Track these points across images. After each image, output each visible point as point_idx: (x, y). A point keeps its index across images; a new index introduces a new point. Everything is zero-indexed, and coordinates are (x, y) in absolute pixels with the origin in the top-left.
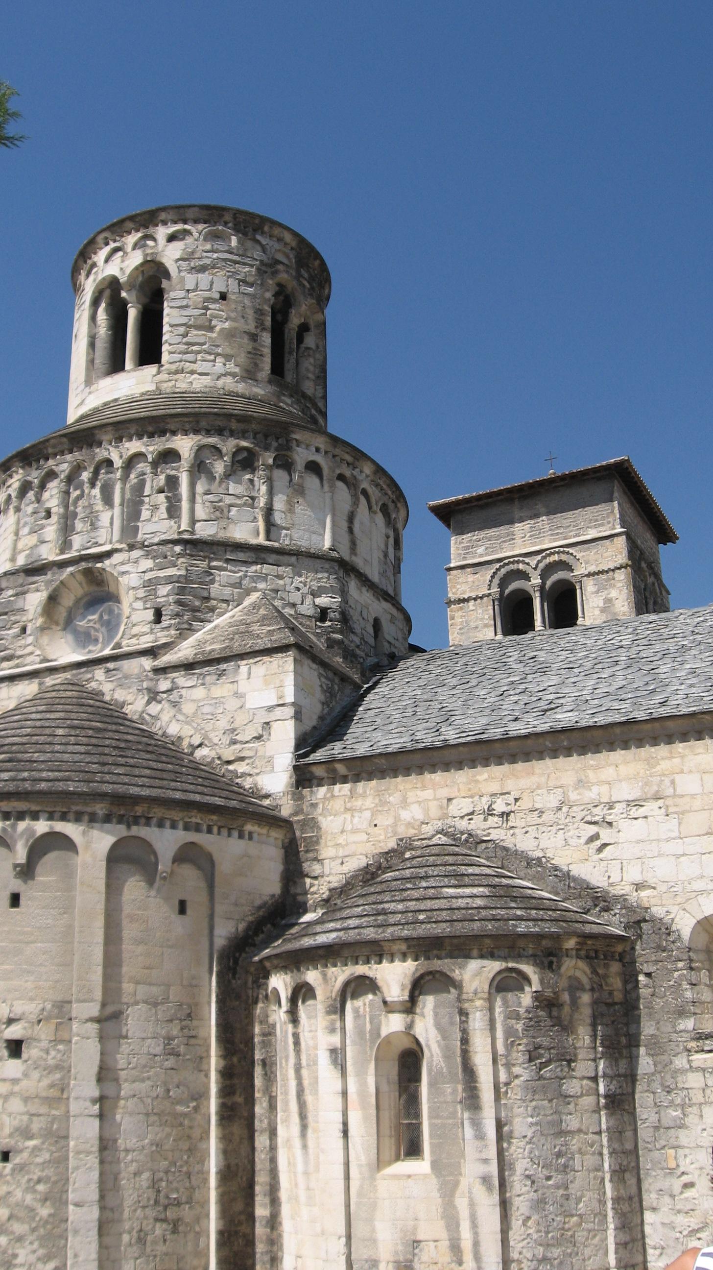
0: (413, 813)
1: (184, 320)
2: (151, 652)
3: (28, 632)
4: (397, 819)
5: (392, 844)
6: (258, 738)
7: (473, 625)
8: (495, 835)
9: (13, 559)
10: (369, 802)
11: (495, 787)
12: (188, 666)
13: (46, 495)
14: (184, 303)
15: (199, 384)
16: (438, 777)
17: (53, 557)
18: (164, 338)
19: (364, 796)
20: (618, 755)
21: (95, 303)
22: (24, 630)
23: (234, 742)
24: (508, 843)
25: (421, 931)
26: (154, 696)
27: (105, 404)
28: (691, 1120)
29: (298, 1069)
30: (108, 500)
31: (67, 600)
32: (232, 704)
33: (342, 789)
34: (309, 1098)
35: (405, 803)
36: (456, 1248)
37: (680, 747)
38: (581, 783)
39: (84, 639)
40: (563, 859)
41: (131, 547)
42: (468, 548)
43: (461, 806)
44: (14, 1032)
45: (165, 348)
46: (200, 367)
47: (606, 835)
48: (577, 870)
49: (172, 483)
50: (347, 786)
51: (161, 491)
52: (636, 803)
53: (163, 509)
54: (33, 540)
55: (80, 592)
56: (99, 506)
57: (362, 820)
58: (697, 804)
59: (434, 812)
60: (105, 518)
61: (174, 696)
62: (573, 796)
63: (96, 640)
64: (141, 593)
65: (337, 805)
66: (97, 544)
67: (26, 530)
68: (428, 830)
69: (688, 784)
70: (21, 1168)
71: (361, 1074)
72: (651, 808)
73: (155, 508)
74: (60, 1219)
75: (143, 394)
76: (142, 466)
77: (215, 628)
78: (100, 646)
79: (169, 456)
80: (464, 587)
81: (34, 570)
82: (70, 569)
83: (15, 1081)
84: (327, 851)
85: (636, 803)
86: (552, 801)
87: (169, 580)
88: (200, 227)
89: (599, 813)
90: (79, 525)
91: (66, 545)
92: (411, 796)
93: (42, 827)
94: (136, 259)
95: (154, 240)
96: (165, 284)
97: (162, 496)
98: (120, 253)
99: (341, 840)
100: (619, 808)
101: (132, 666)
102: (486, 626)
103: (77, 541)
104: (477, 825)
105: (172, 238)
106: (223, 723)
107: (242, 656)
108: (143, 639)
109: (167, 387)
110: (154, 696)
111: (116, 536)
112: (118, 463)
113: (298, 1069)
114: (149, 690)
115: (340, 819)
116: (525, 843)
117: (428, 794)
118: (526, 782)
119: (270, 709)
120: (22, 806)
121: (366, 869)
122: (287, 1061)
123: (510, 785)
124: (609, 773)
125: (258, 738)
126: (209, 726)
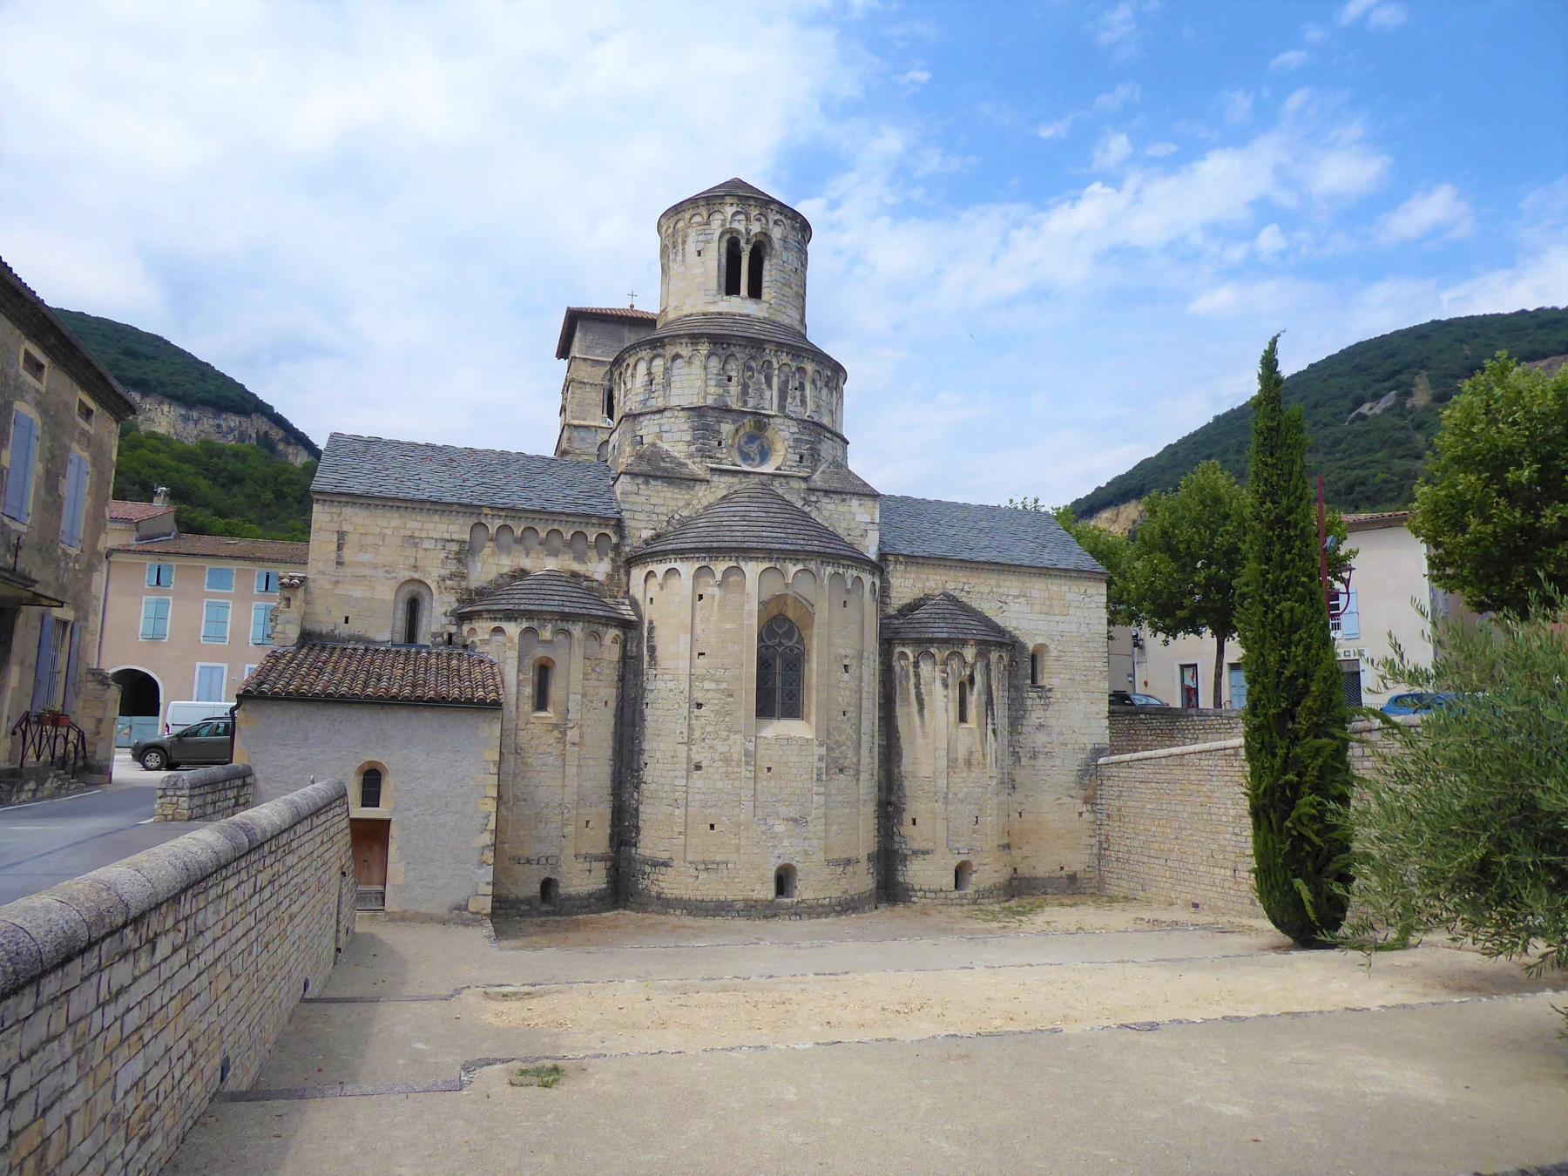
0: (929, 584)
1: (782, 280)
2: (805, 479)
3: (723, 445)
4: (924, 585)
5: (922, 595)
6: (862, 536)
7: (587, 402)
8: (964, 599)
9: (705, 398)
10: (913, 576)
11: (965, 580)
12: (826, 492)
13: (728, 367)
14: (782, 268)
15: (787, 321)
16: (942, 571)
17: (734, 407)
18: (764, 284)
19: (910, 573)
20: (1012, 577)
21: (720, 238)
22: (720, 444)
23: (849, 535)
24: (969, 603)
25: (978, 637)
26: (807, 502)
27: (741, 315)
28: (1027, 716)
29: (917, 686)
30: (770, 386)
31: (741, 433)
32: (848, 516)
33: (901, 568)
34: (926, 699)
35: (928, 580)
36: (983, 754)
37: (1034, 579)
38: (998, 586)
39: (746, 457)
40: (990, 614)
41: (786, 416)
42: (589, 347)
43: (950, 586)
44: (846, 662)
45: (765, 291)
46: (789, 311)
47: (1005, 607)
48: (993, 619)
49: (802, 387)
50: (902, 568)
51: (796, 389)
52: (1016, 597)
53: (798, 399)
54: (721, 391)
55: (747, 430)
56: (764, 386)
57: (909, 583)
58: (1038, 602)
59: (940, 586)
60: (767, 394)
61: (818, 505)
62: (995, 590)
63: (753, 460)
64: (792, 444)
65: (898, 574)
66: (763, 408)
67: (713, 383)
68: (937, 592)
69: (1035, 593)
70: (849, 719)
71: (954, 689)
72: (1022, 600)
73: (794, 398)
74: (859, 740)
75: (765, 318)
76: (786, 369)
77: (823, 472)
78: (756, 463)
79: (801, 370)
80: (582, 374)
81: (724, 411)
82: (749, 417)
83: (847, 683)
84: (893, 594)
85: (1016, 597)
86: (987, 590)
87: (807, 442)
88: (789, 222)
89: (1003, 598)
90: (752, 394)
91: (745, 403)
92: (931, 577)
93: (855, 573)
94: (756, 228)
95: (767, 221)
96: (768, 250)
97: (798, 393)
98: (742, 217)
99: (900, 590)
100: (1010, 598)
101: (795, 484)
102: (596, 405)
103: (751, 402)
104: (956, 594)
105: (775, 222)
106: (844, 525)
107: (853, 494)
108: (794, 469)
109: (773, 317)
110: (807, 502)
111: (775, 406)
112: (776, 365)
113: (917, 686)
114: (804, 499)
115: (899, 581)
116: (975, 605)
117: (936, 577)
118: (976, 581)
119: (867, 523)
120: (849, 563)
121: (910, 604)
122: (908, 682)
123: (971, 580)
124: (1008, 583)
125: (862, 536)
126: (837, 525)
